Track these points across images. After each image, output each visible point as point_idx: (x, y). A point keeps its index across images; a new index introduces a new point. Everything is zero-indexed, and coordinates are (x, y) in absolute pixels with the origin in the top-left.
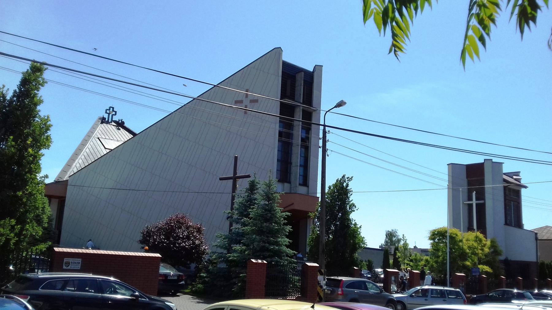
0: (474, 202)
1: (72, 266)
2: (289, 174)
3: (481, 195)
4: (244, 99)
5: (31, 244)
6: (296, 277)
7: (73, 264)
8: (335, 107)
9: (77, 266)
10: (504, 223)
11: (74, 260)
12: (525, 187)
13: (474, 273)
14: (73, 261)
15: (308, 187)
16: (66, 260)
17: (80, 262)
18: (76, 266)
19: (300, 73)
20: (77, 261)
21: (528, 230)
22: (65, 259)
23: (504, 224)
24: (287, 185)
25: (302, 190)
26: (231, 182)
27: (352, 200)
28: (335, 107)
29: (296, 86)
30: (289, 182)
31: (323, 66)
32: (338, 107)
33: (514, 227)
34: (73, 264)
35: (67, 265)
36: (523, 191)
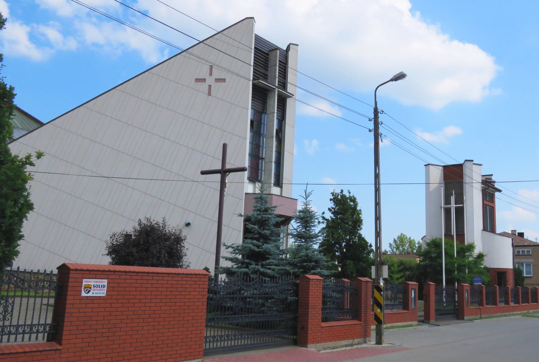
0: (453, 206)
1: (95, 292)
2: (260, 171)
3: (460, 199)
4: (207, 77)
5: (301, 238)
6: (339, 295)
7: (95, 288)
8: (392, 80)
9: (102, 292)
10: (482, 229)
11: (97, 282)
12: (500, 191)
13: (475, 283)
14: (96, 284)
15: (281, 187)
16: (85, 282)
17: (106, 284)
18: (99, 292)
19: (274, 51)
20: (101, 284)
21: (507, 237)
22: (84, 280)
23: (482, 230)
24: (258, 185)
25: (275, 190)
26: (219, 176)
27: (312, 207)
28: (392, 80)
29: (269, 65)
30: (260, 181)
31: (298, 45)
32: (395, 81)
33: (489, 232)
34: (95, 288)
35: (87, 290)
36: (497, 194)
